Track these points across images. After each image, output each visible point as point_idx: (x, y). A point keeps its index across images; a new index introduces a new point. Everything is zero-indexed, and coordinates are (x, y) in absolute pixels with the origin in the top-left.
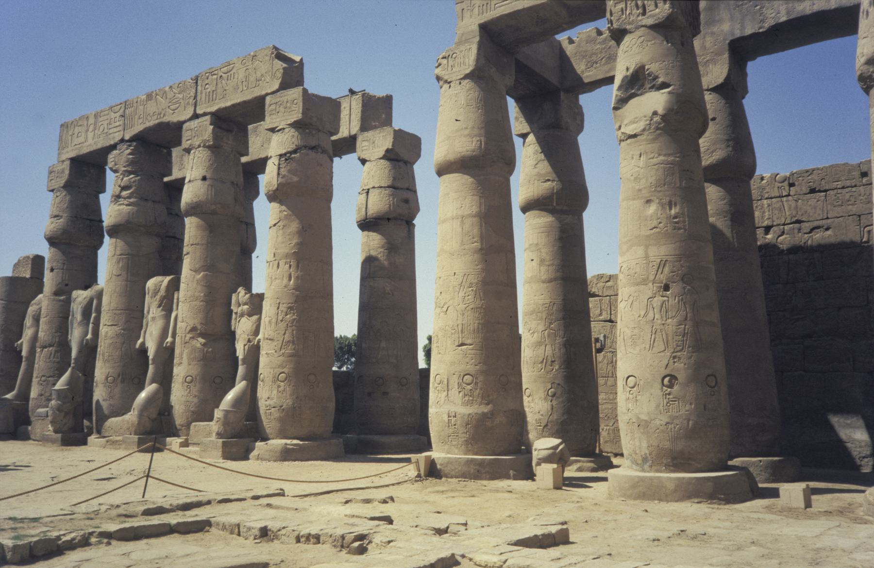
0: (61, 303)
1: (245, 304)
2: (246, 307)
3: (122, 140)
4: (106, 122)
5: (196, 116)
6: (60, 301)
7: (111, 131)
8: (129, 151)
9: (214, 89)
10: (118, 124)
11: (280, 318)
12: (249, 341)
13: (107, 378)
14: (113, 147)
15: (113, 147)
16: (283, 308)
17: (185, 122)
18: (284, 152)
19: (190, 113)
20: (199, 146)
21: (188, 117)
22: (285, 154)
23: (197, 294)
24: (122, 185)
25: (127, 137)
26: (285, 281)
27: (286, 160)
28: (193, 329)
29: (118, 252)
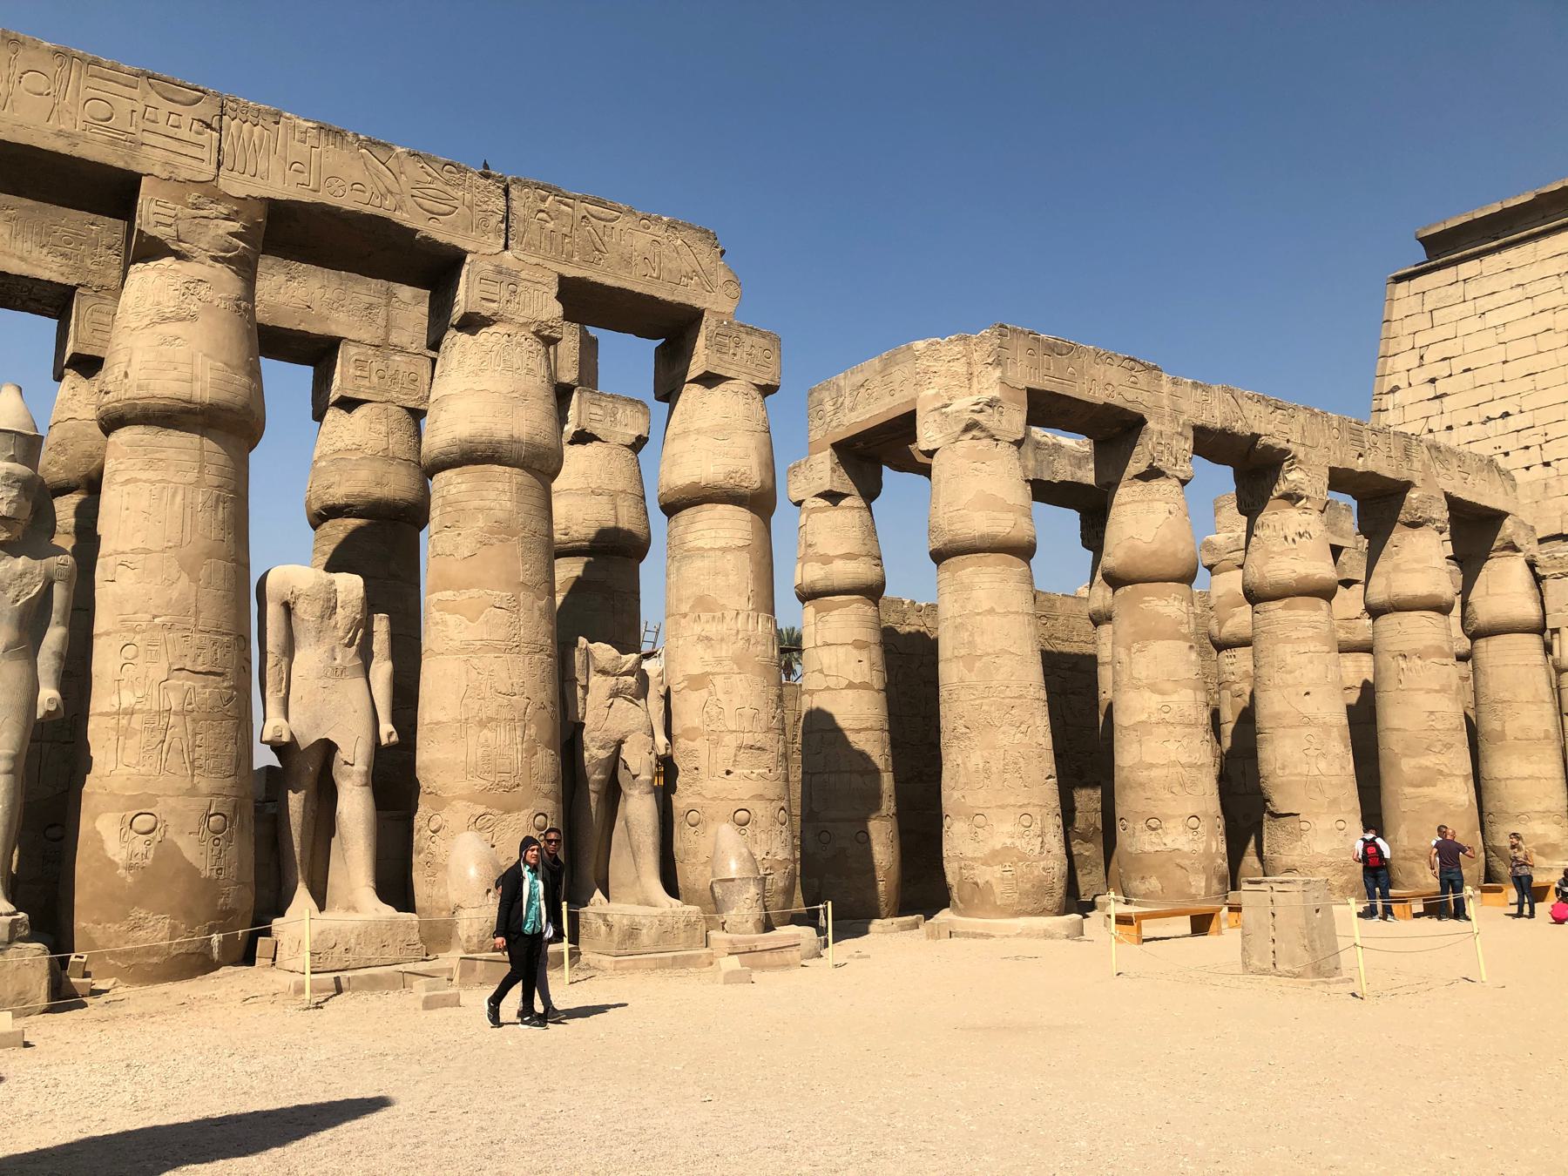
4: (127, 106)
7: (150, 138)
8: (235, 226)
9: (566, 230)
10: (184, 133)
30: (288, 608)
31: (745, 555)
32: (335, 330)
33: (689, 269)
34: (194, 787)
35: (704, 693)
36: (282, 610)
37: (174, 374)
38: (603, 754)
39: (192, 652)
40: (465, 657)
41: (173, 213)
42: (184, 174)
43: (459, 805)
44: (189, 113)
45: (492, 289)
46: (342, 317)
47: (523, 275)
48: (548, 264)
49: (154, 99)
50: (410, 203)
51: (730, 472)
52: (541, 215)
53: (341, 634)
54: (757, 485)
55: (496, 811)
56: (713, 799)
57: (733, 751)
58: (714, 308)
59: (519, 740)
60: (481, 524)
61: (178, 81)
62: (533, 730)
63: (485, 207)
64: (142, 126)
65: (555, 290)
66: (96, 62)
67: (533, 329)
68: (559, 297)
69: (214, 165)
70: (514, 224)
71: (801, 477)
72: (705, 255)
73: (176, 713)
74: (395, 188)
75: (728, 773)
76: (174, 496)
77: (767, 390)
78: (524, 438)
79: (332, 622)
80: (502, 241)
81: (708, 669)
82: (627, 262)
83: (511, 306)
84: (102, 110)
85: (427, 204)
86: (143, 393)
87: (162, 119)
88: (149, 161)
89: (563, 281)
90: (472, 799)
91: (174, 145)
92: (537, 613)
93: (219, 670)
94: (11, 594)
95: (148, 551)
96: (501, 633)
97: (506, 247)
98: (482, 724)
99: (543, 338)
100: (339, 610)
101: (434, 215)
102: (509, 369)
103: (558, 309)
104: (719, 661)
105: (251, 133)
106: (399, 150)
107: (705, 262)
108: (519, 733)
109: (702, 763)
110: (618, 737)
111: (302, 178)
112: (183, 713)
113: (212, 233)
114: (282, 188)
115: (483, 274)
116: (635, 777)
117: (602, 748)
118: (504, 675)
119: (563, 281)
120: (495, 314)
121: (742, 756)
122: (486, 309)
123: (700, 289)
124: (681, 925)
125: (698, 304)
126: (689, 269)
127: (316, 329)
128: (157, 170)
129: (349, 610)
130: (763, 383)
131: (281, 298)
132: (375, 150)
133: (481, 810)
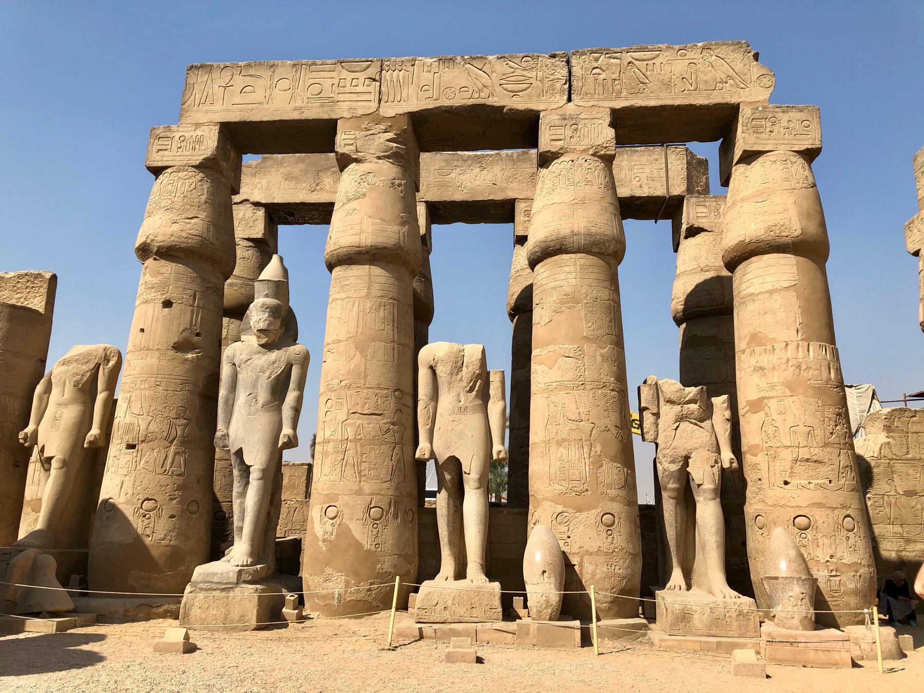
2: (694, 407)
4: (329, 82)
6: (186, 360)
7: (342, 97)
8: (390, 135)
9: (614, 76)
10: (360, 89)
12: (716, 462)
23: (604, 379)
30: (432, 369)
31: (792, 295)
32: (510, 195)
33: (723, 76)
34: (360, 488)
35: (761, 415)
36: (429, 372)
37: (351, 232)
38: (674, 467)
39: (361, 402)
40: (546, 395)
41: (353, 137)
42: (360, 112)
43: (546, 504)
44: (362, 76)
45: (559, 132)
46: (515, 185)
47: (582, 116)
48: (601, 104)
49: (345, 74)
50: (499, 89)
51: (769, 227)
52: (594, 71)
53: (465, 384)
54: (798, 232)
55: (570, 510)
56: (774, 506)
57: (789, 464)
58: (749, 100)
59: (586, 455)
60: (554, 298)
61: (357, 60)
62: (598, 448)
63: (552, 77)
64: (337, 92)
65: (608, 120)
66: (314, 64)
67: (591, 152)
68: (612, 125)
69: (377, 101)
70: (574, 83)
71: (915, 231)
72: (738, 61)
73: (351, 441)
74: (487, 82)
75: (786, 483)
76: (353, 306)
77: (810, 155)
78: (582, 231)
79: (459, 377)
80: (566, 97)
81: (763, 394)
82: (667, 85)
83: (574, 140)
84: (315, 89)
85: (510, 87)
86: (336, 247)
87: (348, 84)
88: (341, 111)
89: (614, 112)
90: (555, 500)
91: (354, 97)
92: (599, 359)
93: (380, 412)
94: (267, 374)
95: (339, 341)
96: (570, 375)
97: (569, 100)
98: (559, 444)
99: (602, 158)
100: (464, 368)
101: (515, 93)
102: (574, 184)
103: (611, 133)
104: (772, 387)
105: (398, 76)
106: (491, 58)
107: (738, 66)
108: (586, 450)
109: (764, 474)
110: (684, 453)
111: (429, 94)
112: (355, 440)
113: (377, 143)
114: (415, 104)
115: (552, 123)
116: (699, 486)
117: (673, 462)
118: (573, 406)
119: (614, 112)
120: (561, 149)
121: (799, 468)
122: (554, 147)
123: (734, 89)
124: (734, 615)
125: (734, 100)
126: (723, 76)
127: (498, 196)
128: (346, 114)
129: (470, 369)
130: (803, 148)
131: (478, 183)
132: (474, 63)
133: (560, 508)
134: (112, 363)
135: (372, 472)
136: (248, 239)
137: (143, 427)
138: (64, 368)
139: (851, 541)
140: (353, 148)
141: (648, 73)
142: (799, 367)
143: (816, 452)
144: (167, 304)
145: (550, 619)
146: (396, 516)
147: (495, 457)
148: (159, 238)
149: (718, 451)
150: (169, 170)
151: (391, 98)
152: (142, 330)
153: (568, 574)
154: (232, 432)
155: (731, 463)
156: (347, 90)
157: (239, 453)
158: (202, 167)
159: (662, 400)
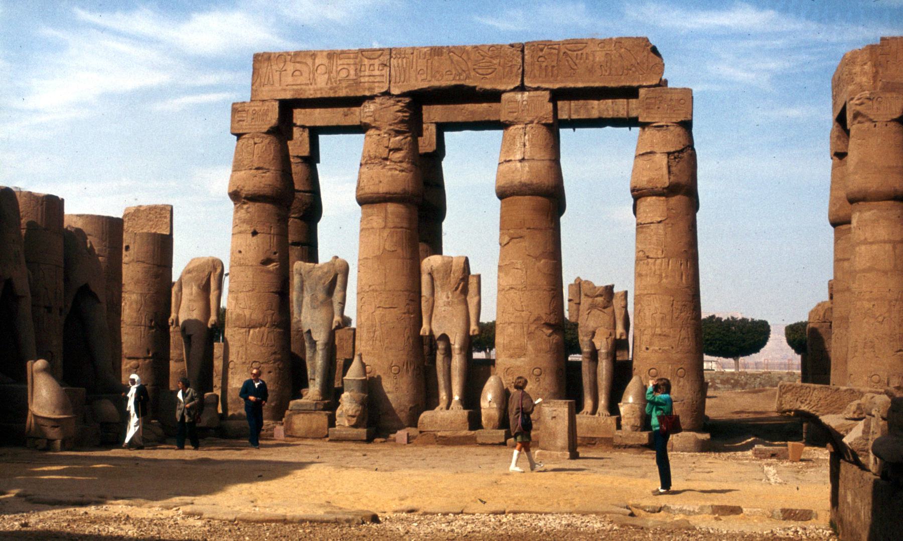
0: (271, 275)
1: (601, 295)
2: (600, 299)
3: (387, 94)
5: (522, 88)
6: (269, 272)
8: (398, 108)
10: (377, 73)
11: (676, 315)
13: (391, 367)
14: (372, 98)
15: (372, 98)
16: (678, 305)
17: (505, 91)
18: (672, 150)
19: (518, 84)
20: (532, 122)
21: (512, 87)
22: (674, 153)
24: (391, 146)
25: (395, 91)
26: (678, 279)
27: (675, 158)
28: (538, 319)
29: (390, 225)
50: (473, 73)
67: (536, 121)
91: (372, 79)
111: (424, 77)
130: (679, 120)
134: (219, 270)
135: (393, 345)
136: (298, 157)
137: (248, 316)
138: (190, 275)
139: (681, 384)
140: (372, 119)
141: (577, 61)
142: (661, 275)
143: (666, 330)
144: (255, 233)
145: (494, 428)
146: (407, 371)
147: (471, 333)
148: (246, 188)
149: (615, 327)
150: (247, 136)
151: (398, 80)
152: (240, 252)
153: (371, 389)
154: (302, 318)
155: (621, 336)
156: (367, 73)
157: (309, 332)
158: (268, 132)
159: (582, 294)
